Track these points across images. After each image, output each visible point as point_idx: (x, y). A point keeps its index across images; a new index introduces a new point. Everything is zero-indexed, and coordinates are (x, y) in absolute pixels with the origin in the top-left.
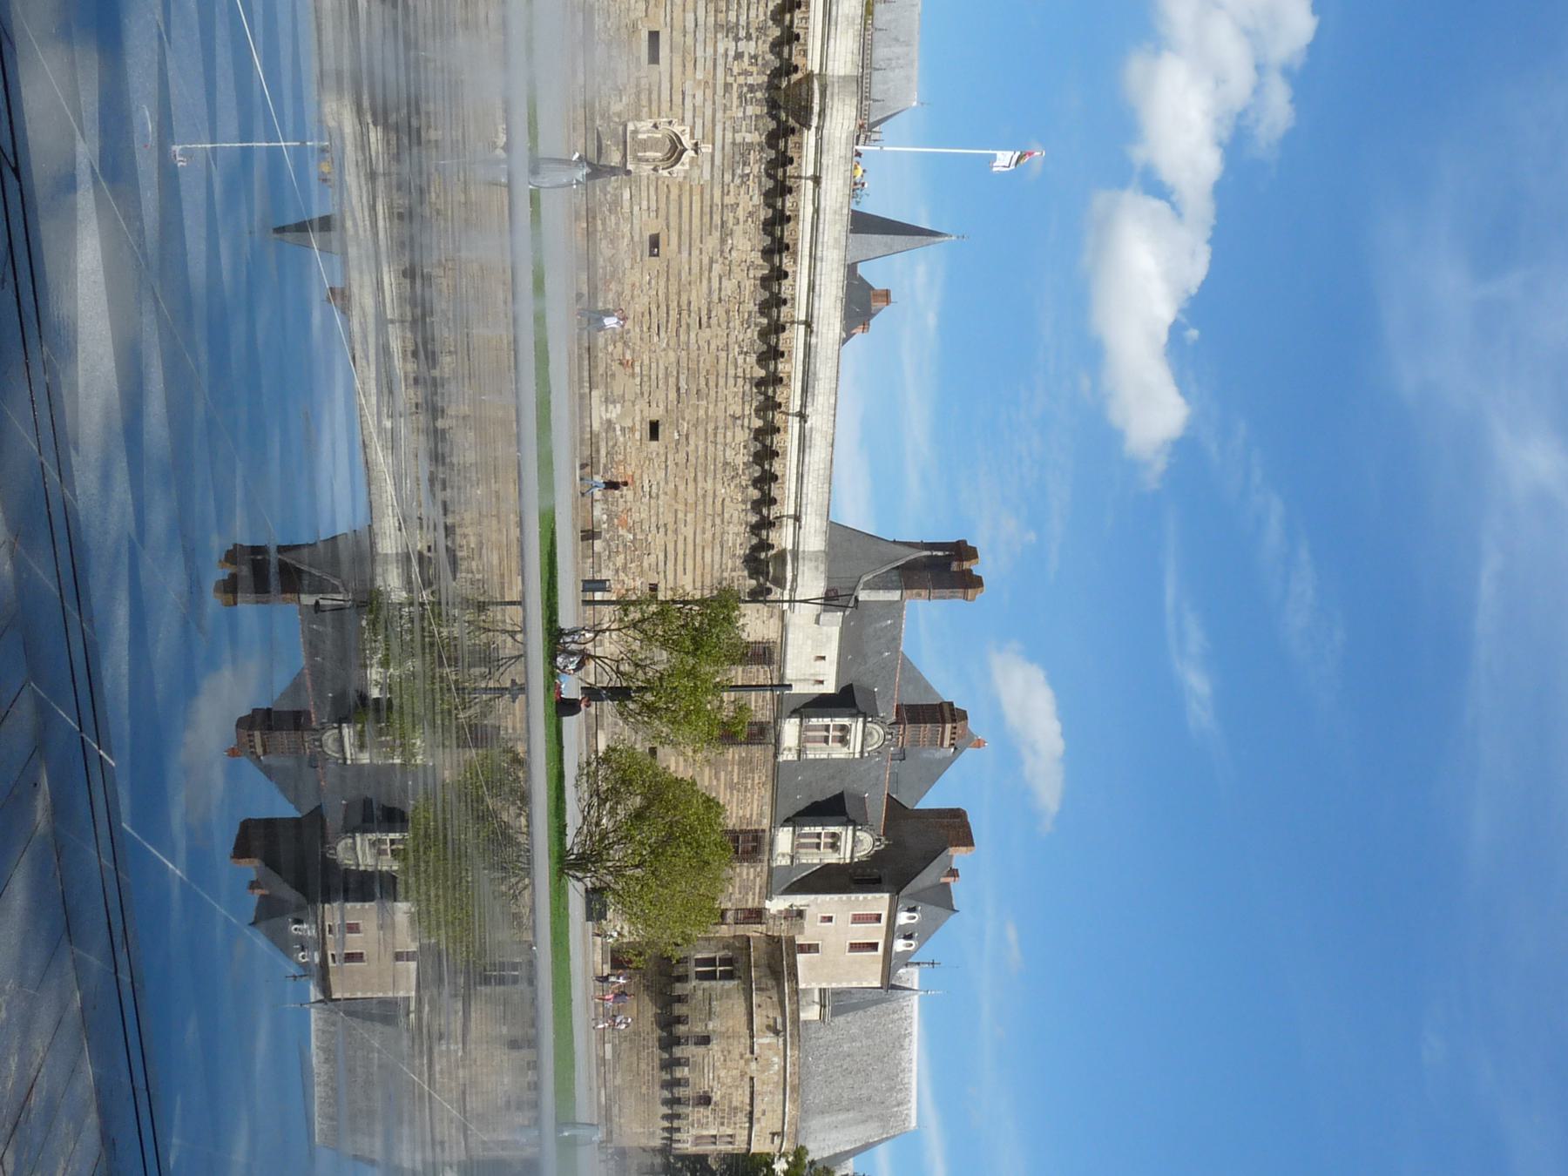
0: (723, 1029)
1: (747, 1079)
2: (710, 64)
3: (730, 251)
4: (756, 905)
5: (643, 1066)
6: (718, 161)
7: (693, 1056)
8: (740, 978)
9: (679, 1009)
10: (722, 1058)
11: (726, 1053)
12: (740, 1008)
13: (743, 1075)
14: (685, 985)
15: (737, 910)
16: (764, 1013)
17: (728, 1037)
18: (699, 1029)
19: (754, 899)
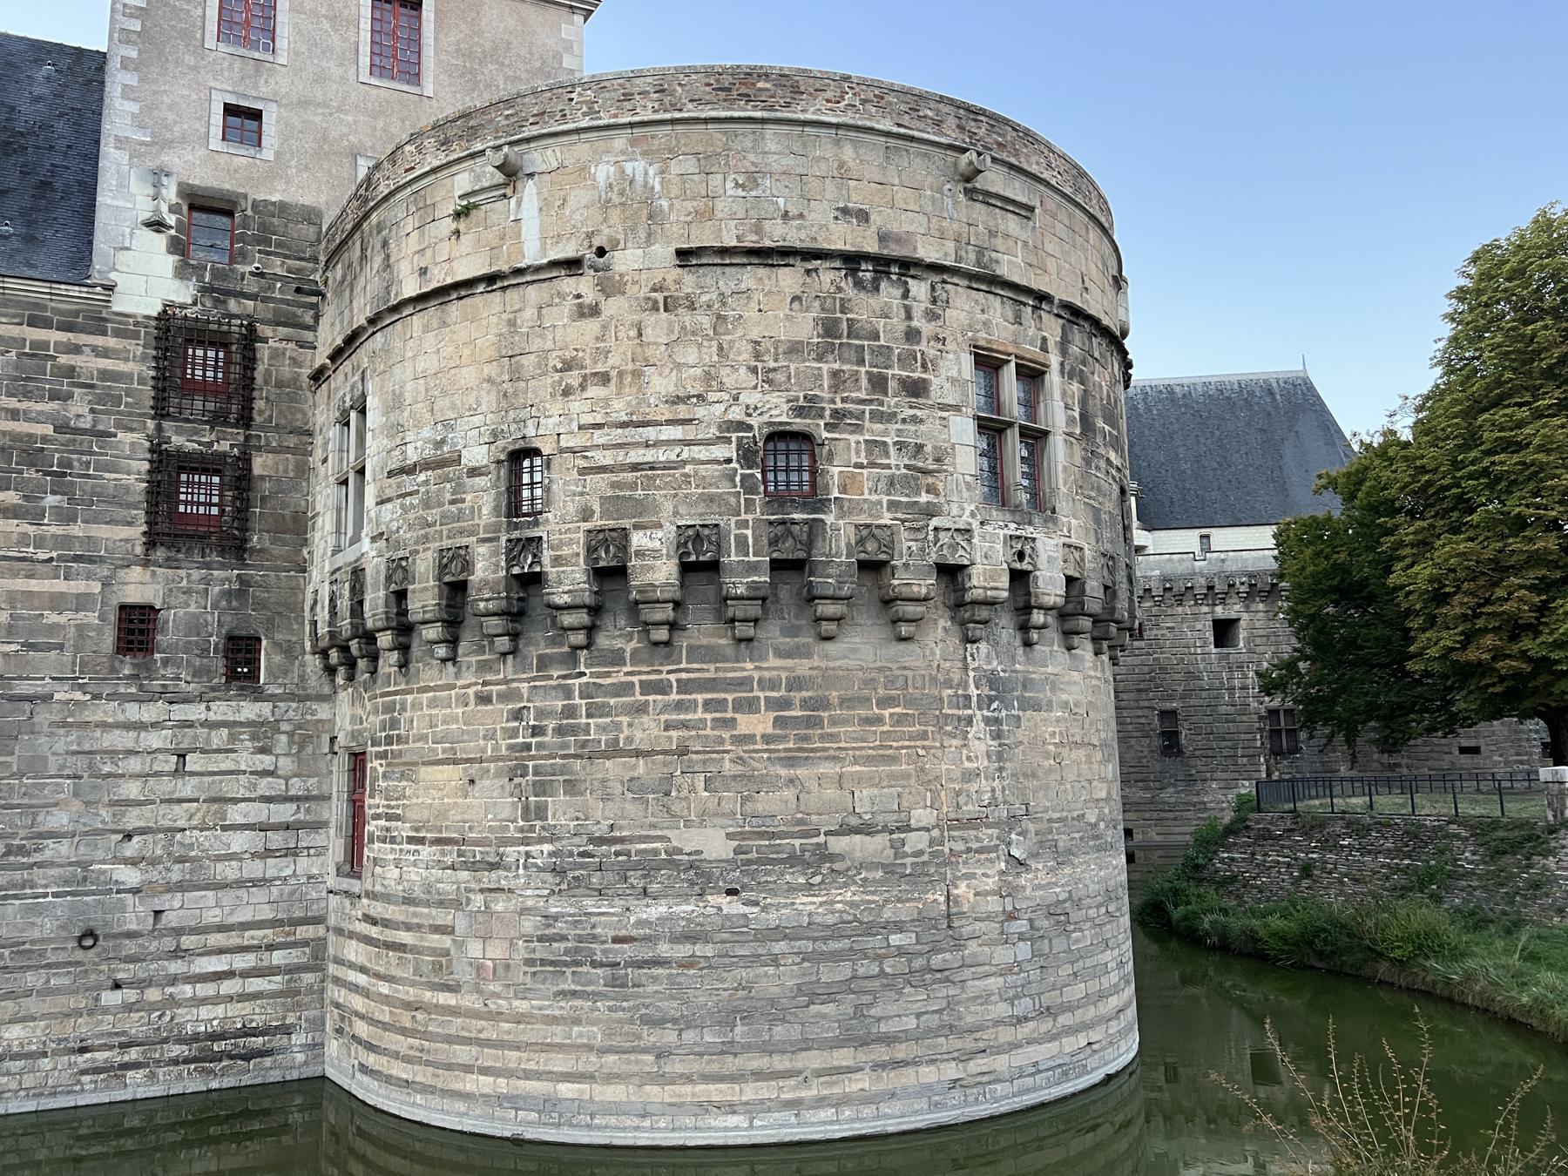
0: (489, 400)
1: (689, 281)
4: (136, 348)
7: (586, 514)
10: (594, 391)
15: (161, 411)
16: (445, 249)
17: (516, 376)
18: (484, 500)
19: (104, 353)
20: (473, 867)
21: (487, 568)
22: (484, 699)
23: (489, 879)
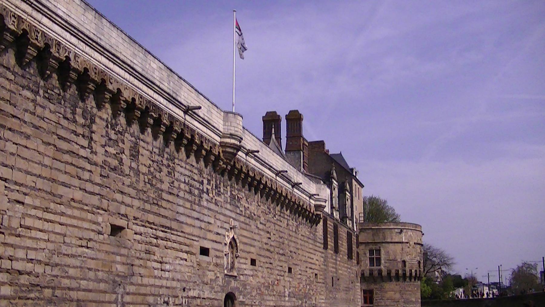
2: (210, 213)
3: (255, 215)
5: (410, 289)
6: (233, 215)
8: (380, 247)
9: (393, 274)
11: (408, 254)
12: (391, 246)
13: (414, 248)
14: (383, 271)
18: (400, 265)
20: (396, 302)
21: (400, 272)
22: (396, 285)
23: (398, 303)
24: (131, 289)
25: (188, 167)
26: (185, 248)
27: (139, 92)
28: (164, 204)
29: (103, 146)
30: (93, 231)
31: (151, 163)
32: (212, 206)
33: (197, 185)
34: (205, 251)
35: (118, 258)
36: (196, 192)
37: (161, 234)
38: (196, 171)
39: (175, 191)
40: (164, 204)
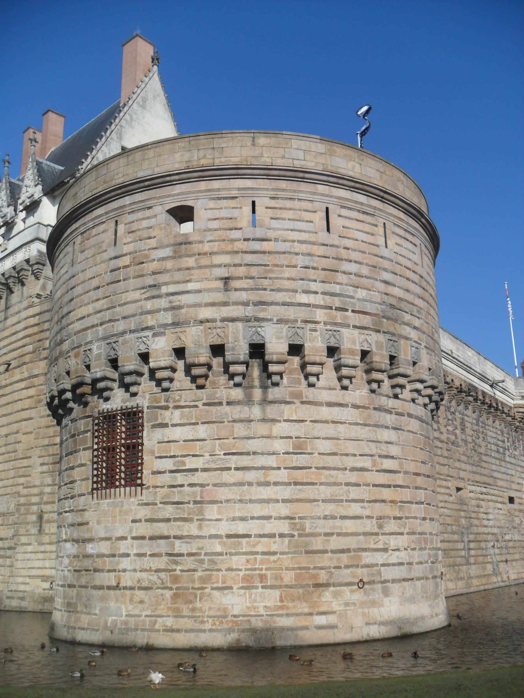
24: (472, 537)
25: (494, 430)
26: (500, 499)
27: (463, 377)
28: (484, 464)
29: (445, 426)
30: (447, 494)
31: (473, 432)
32: (513, 460)
33: (500, 443)
34: (511, 500)
35: (462, 514)
36: (501, 450)
37: (484, 490)
38: (499, 432)
39: (489, 452)
40: (484, 464)
